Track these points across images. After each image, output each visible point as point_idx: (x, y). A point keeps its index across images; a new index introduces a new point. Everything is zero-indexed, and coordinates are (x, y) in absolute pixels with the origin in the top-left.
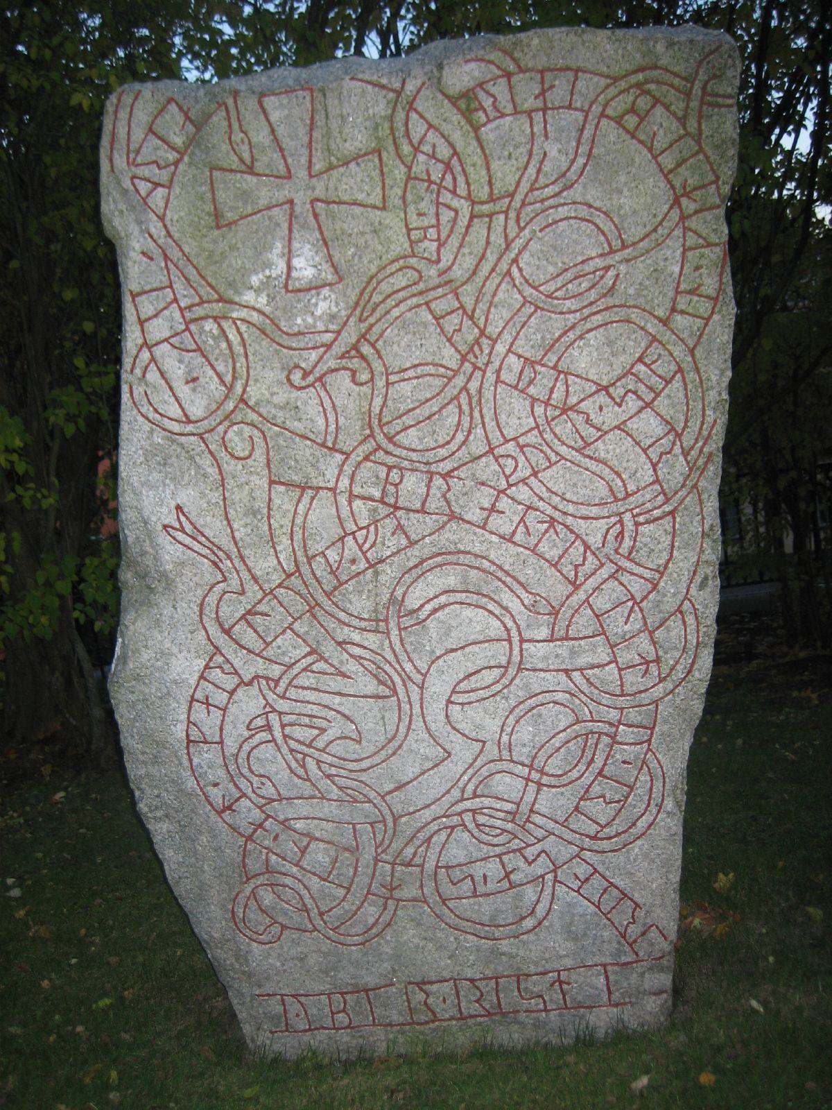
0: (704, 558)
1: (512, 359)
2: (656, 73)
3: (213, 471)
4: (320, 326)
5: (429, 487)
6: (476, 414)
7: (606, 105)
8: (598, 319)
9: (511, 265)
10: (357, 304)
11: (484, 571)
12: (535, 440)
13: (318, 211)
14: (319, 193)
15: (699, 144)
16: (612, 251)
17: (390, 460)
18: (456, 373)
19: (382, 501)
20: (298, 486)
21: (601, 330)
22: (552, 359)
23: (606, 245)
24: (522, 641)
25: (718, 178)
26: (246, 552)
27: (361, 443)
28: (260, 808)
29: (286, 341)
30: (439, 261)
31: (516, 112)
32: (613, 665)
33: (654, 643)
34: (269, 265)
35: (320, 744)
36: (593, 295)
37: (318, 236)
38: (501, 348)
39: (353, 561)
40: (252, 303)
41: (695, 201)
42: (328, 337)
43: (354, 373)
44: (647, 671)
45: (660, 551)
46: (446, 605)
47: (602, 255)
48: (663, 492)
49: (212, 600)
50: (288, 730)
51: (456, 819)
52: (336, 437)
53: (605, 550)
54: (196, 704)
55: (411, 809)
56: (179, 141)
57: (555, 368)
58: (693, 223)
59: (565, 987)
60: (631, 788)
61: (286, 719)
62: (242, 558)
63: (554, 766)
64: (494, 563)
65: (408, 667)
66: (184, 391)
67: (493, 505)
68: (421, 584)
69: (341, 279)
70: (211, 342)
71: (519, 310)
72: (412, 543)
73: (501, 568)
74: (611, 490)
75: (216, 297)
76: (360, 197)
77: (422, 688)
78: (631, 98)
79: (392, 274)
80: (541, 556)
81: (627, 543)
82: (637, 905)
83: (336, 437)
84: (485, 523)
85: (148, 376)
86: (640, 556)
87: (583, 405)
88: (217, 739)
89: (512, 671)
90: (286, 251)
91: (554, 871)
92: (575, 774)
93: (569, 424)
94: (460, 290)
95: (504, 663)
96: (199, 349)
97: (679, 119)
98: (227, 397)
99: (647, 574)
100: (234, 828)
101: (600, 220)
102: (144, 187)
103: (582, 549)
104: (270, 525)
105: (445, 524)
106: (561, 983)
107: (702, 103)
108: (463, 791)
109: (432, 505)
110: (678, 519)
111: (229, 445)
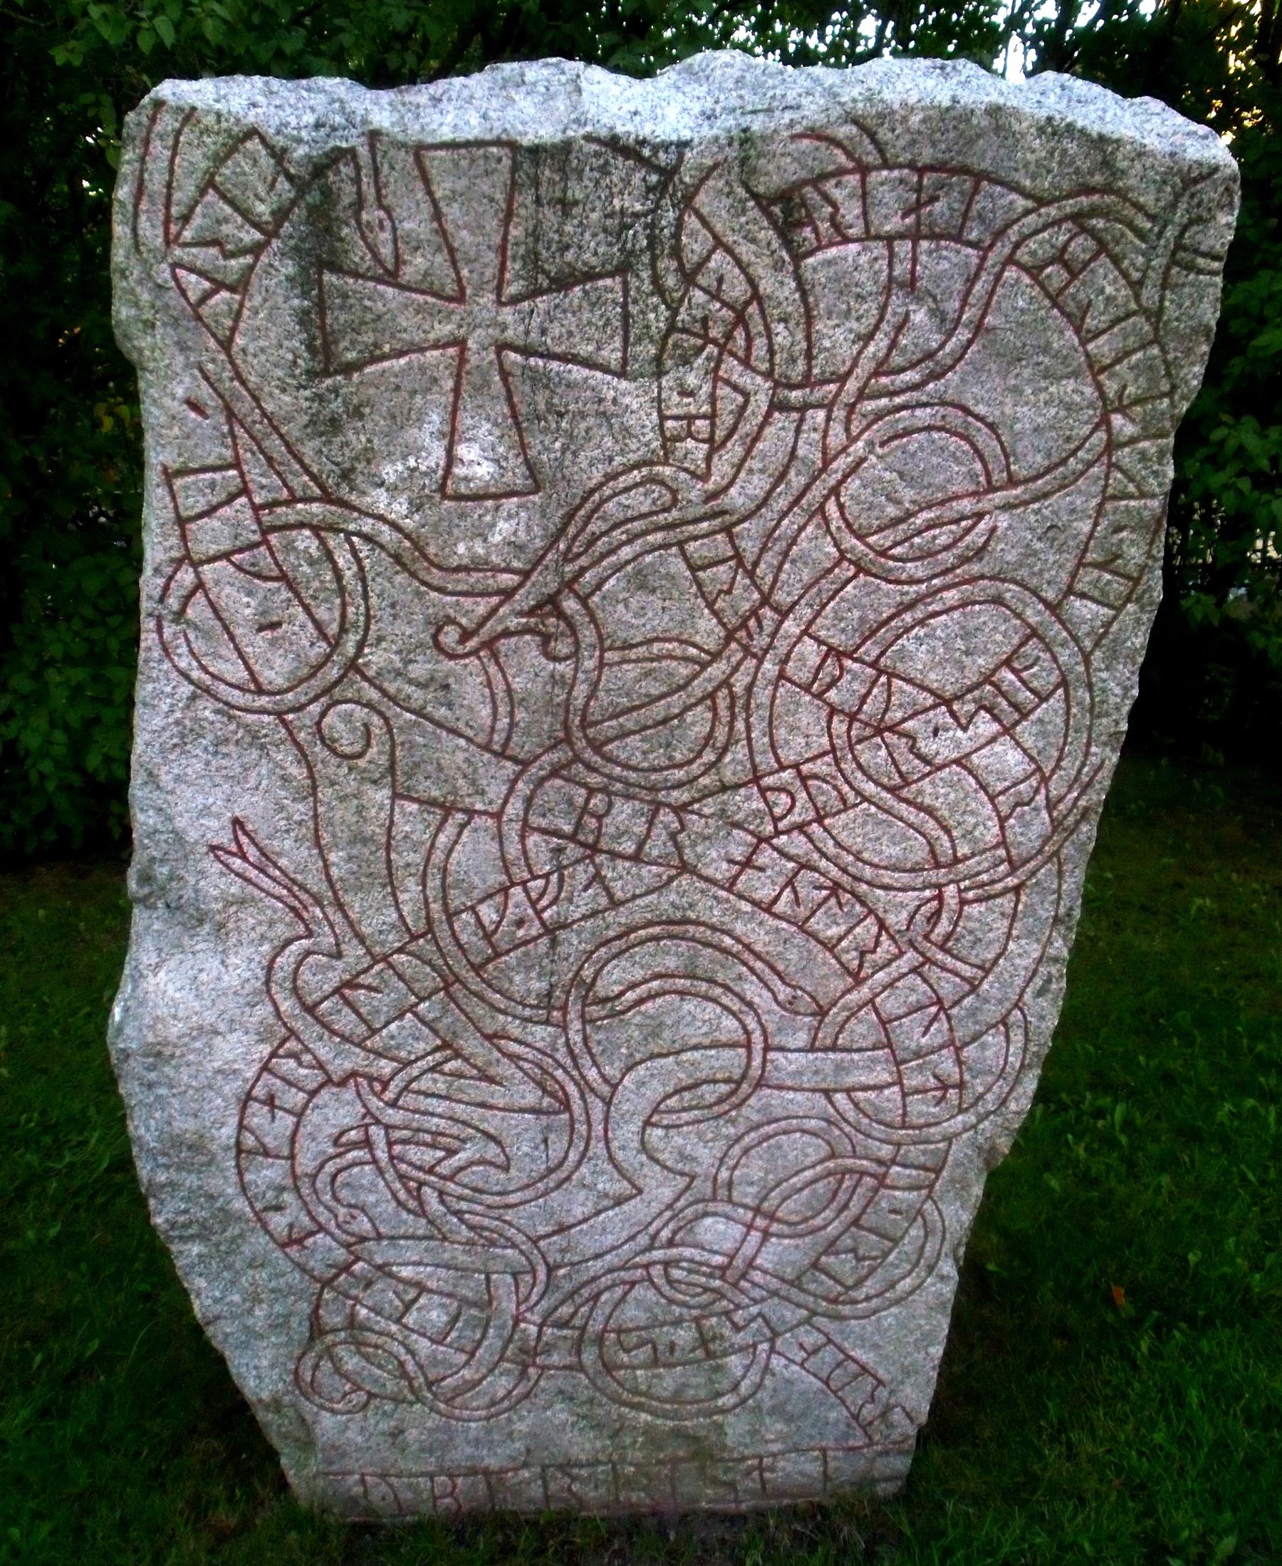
0: (1052, 951)
1: (808, 645)
2: (1110, 199)
4: (495, 559)
5: (651, 823)
6: (740, 725)
7: (1017, 246)
8: (952, 596)
10: (562, 531)
11: (725, 951)
13: (507, 367)
15: (1156, 329)
16: (991, 489)
17: (594, 780)
18: (715, 656)
19: (572, 837)
20: (442, 806)
21: (956, 614)
22: (870, 650)
24: (767, 1049)
25: (1174, 388)
26: (346, 898)
27: (552, 748)
28: (348, 1246)
29: (436, 576)
30: (705, 477)
31: (868, 236)
32: (896, 1089)
33: (959, 1062)
34: (417, 450)
35: (444, 1169)
36: (948, 558)
37: (506, 410)
38: (791, 627)
39: (520, 923)
40: (381, 508)
41: (1133, 421)
42: (507, 579)
43: (546, 639)
44: (943, 1097)
45: (990, 942)
47: (974, 494)
49: (286, 961)
50: (397, 1149)
51: (639, 1273)
52: (508, 738)
53: (910, 934)
54: (255, 1106)
57: (873, 665)
58: (1124, 456)
60: (896, 1242)
61: (397, 1134)
62: (340, 907)
63: (789, 1210)
64: (738, 940)
65: (592, 1074)
66: (256, 644)
70: (306, 569)
71: (830, 571)
72: (615, 904)
73: (748, 947)
74: (933, 852)
76: (586, 349)
77: (608, 1103)
78: (1063, 238)
79: (627, 490)
80: (813, 935)
81: (943, 927)
82: (880, 1382)
83: (508, 738)
84: (733, 884)
85: (190, 612)
86: (962, 947)
87: (909, 725)
88: (286, 1152)
90: (447, 429)
91: (772, 1341)
92: (818, 1221)
93: (883, 752)
94: (737, 529)
96: (283, 577)
98: (328, 658)
100: (303, 1269)
101: (983, 438)
103: (875, 929)
104: (389, 861)
105: (671, 879)
107: (1173, 261)
108: (654, 1237)
109: (654, 849)
111: (326, 731)
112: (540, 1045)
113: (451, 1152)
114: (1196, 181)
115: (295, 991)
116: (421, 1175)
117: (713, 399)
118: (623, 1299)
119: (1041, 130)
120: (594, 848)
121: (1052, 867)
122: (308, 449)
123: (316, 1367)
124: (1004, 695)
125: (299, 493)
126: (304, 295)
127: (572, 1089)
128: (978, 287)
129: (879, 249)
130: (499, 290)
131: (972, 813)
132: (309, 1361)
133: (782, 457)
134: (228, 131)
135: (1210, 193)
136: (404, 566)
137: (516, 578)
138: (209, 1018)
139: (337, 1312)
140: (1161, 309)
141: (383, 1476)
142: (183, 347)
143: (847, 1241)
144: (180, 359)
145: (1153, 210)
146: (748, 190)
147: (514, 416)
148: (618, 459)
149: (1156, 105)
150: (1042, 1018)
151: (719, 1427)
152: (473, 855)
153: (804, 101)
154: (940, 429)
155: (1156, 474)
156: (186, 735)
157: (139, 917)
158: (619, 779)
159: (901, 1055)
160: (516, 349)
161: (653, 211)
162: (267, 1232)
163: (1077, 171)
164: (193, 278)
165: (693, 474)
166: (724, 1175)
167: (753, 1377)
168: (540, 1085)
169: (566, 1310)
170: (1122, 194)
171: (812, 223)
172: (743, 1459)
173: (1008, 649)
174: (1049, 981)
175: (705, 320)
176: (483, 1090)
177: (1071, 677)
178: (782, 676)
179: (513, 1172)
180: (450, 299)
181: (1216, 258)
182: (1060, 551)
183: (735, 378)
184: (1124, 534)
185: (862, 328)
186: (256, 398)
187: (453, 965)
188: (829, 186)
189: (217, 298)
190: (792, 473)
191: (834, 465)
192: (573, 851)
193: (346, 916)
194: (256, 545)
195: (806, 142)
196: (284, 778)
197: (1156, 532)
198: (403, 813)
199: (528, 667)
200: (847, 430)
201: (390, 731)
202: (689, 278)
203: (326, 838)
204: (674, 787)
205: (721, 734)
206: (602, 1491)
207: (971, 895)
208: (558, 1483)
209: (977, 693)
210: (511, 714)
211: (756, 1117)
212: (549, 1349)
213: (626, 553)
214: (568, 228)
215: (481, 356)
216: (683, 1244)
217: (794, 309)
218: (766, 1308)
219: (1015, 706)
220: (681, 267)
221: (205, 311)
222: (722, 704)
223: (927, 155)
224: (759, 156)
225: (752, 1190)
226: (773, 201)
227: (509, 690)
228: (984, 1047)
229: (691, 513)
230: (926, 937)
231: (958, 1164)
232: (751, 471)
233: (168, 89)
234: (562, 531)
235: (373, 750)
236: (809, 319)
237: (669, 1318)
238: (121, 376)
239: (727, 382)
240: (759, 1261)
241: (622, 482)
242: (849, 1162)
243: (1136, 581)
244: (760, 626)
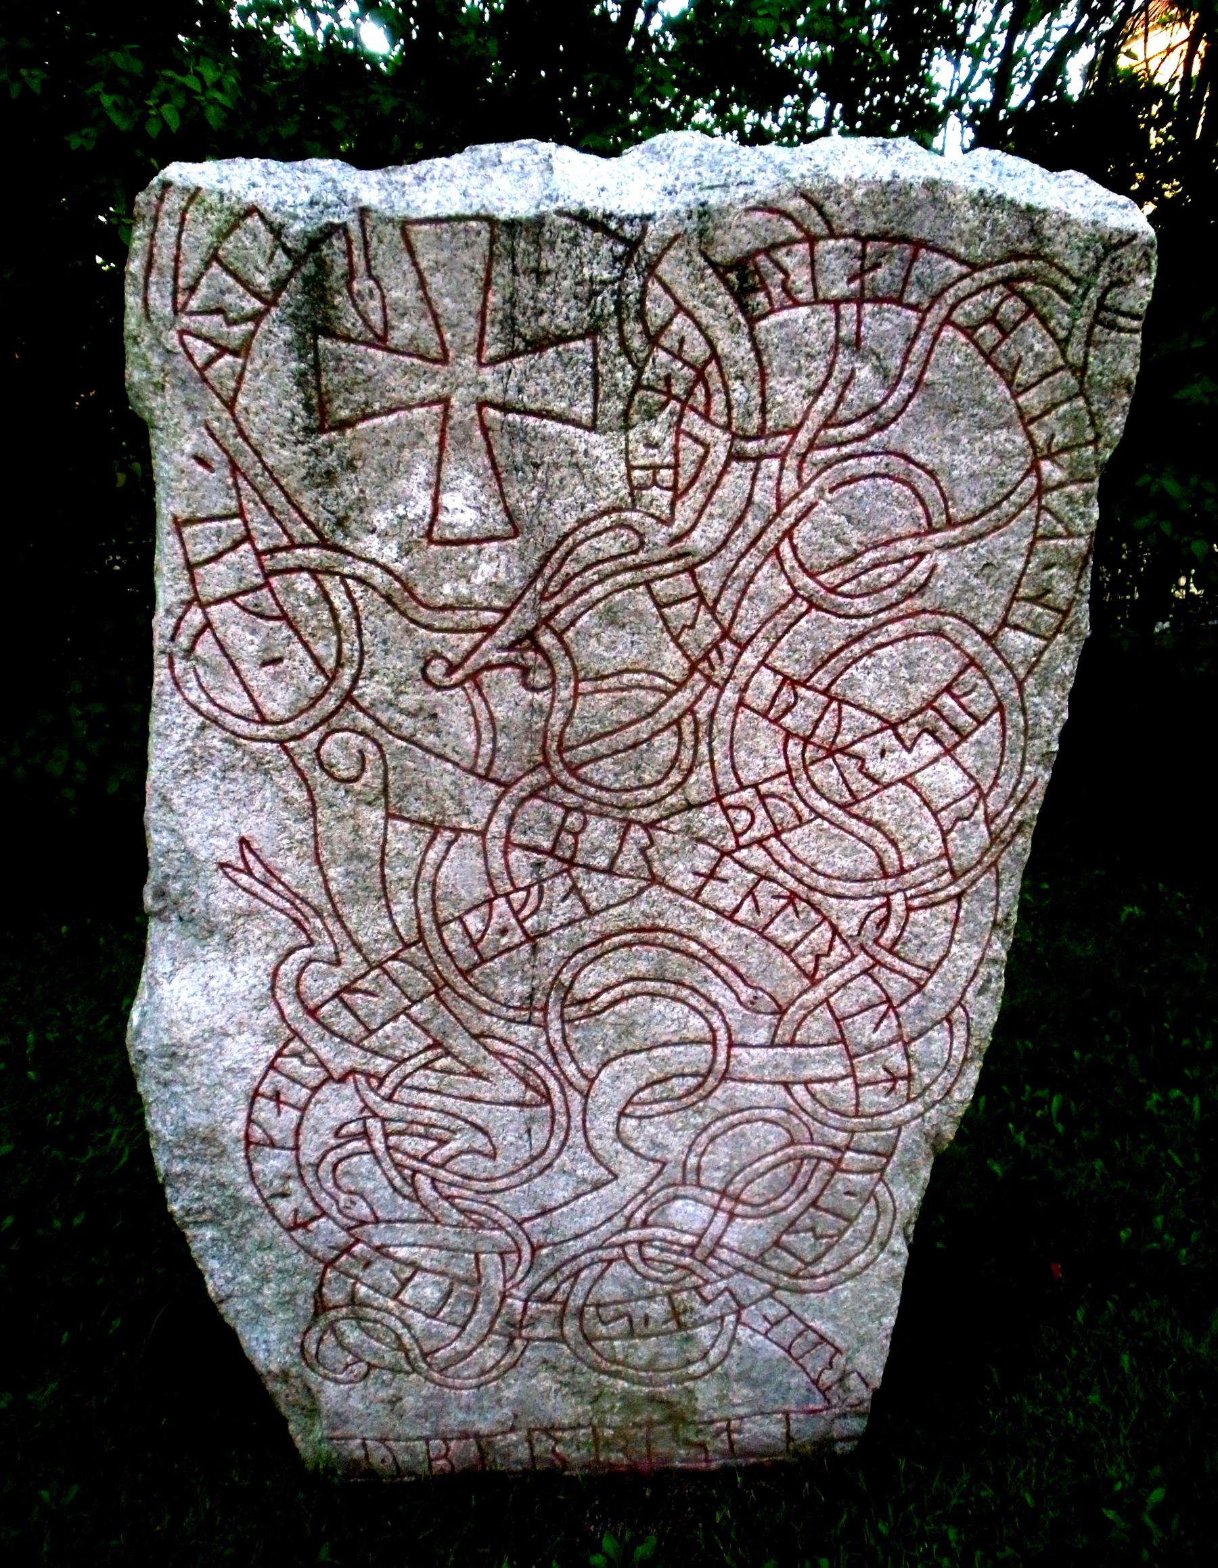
0: (990, 954)
1: (765, 676)
2: (1036, 264)
3: (299, 795)
4: (478, 598)
5: (623, 839)
6: (703, 749)
7: (953, 308)
9: (781, 540)
10: (538, 572)
11: (692, 956)
12: (782, 789)
15: (1081, 383)
16: (932, 530)
17: (570, 800)
18: (680, 686)
19: (551, 853)
20: (431, 825)
21: (901, 645)
22: (822, 679)
23: (923, 521)
24: (731, 1045)
25: (1098, 437)
26: (344, 910)
28: (348, 1229)
29: (424, 615)
30: (669, 522)
31: (817, 300)
32: (850, 1081)
33: (907, 1056)
35: (436, 1158)
36: (893, 594)
37: (487, 462)
38: (749, 658)
39: (504, 932)
40: (373, 554)
41: (1060, 467)
42: (489, 617)
43: (525, 671)
44: (893, 1089)
46: (630, 996)
48: (952, 870)
49: (289, 968)
50: (393, 1140)
51: (616, 1252)
52: (491, 763)
56: (263, 281)
57: (825, 692)
60: (850, 1221)
62: (339, 918)
64: (704, 946)
65: (571, 1069)
66: (259, 678)
67: (713, 871)
69: (516, 534)
70: (305, 609)
71: (784, 607)
72: (590, 913)
73: (712, 952)
74: (881, 864)
75: (315, 538)
76: (559, 406)
79: (598, 534)
80: (771, 940)
81: (892, 932)
82: (838, 1350)
83: (491, 763)
85: (199, 650)
86: (908, 950)
87: (858, 748)
88: (291, 1144)
90: (432, 479)
91: (738, 1313)
92: (780, 1203)
93: (835, 772)
94: (699, 570)
96: (284, 616)
97: (1058, 342)
98: (326, 690)
100: (308, 1251)
101: (923, 483)
102: (203, 352)
103: (829, 935)
104: (383, 876)
105: (641, 890)
107: (1096, 320)
108: (629, 1219)
109: (626, 862)
110: (965, 905)
111: (324, 758)
112: (523, 1043)
113: (442, 1142)
115: (298, 994)
116: (415, 1164)
117: (676, 450)
118: (601, 1276)
119: (974, 202)
120: (571, 863)
122: (306, 499)
123: (320, 1341)
124: (944, 718)
125: (298, 540)
126: (301, 358)
127: (552, 1084)
128: (918, 346)
129: (827, 312)
130: (479, 351)
131: (917, 827)
132: (314, 1334)
133: (739, 503)
134: (230, 209)
135: (1129, 258)
136: (394, 605)
137: (498, 616)
138: (220, 1021)
139: (340, 1290)
140: (1086, 364)
141: (383, 1440)
142: (190, 407)
143: (806, 1221)
144: (188, 419)
145: (1076, 272)
146: (707, 259)
147: (494, 466)
148: (589, 506)
149: (1079, 178)
150: (983, 1015)
151: (690, 1392)
152: (461, 870)
153: (758, 177)
154: (884, 476)
155: (1082, 515)
156: (197, 761)
157: (155, 929)
158: (592, 799)
159: (854, 1049)
160: (495, 406)
161: (620, 279)
162: (274, 1217)
163: (1007, 239)
164: (199, 343)
165: (659, 520)
166: (693, 1160)
167: (721, 1346)
168: (523, 1080)
169: (548, 1287)
170: (1049, 260)
171: (765, 288)
172: (712, 1422)
173: (949, 677)
174: (989, 981)
175: (668, 379)
176: (472, 1085)
177: (1006, 702)
178: (741, 703)
179: (499, 1160)
181: (1135, 317)
182: (995, 587)
183: (696, 431)
184: (1054, 571)
185: (812, 384)
186: (257, 453)
187: (444, 972)
188: (780, 255)
189: (221, 362)
190: (749, 518)
191: (788, 510)
192: (551, 865)
193: (344, 927)
194: (258, 588)
195: (759, 214)
196: (286, 801)
197: (1083, 569)
198: (396, 832)
199: (508, 696)
200: (799, 477)
201: (383, 757)
202: (653, 339)
203: (325, 856)
205: (686, 757)
206: (584, 1452)
207: (916, 902)
208: (543, 1445)
209: (920, 717)
210: (494, 740)
211: (721, 1108)
213: (598, 591)
214: (542, 295)
215: (462, 413)
216: (655, 1225)
221: (210, 373)
222: (687, 729)
223: (869, 225)
224: (716, 228)
225: (720, 1174)
227: (492, 718)
228: (929, 1041)
229: (657, 555)
230: (876, 941)
231: (907, 1150)
232: (711, 516)
233: (176, 172)
234: (538, 572)
235: (368, 775)
236: (763, 376)
238: (135, 435)
239: (689, 435)
240: (725, 1240)
241: (594, 527)
242: (807, 1148)
243: (1065, 614)
244: (721, 657)
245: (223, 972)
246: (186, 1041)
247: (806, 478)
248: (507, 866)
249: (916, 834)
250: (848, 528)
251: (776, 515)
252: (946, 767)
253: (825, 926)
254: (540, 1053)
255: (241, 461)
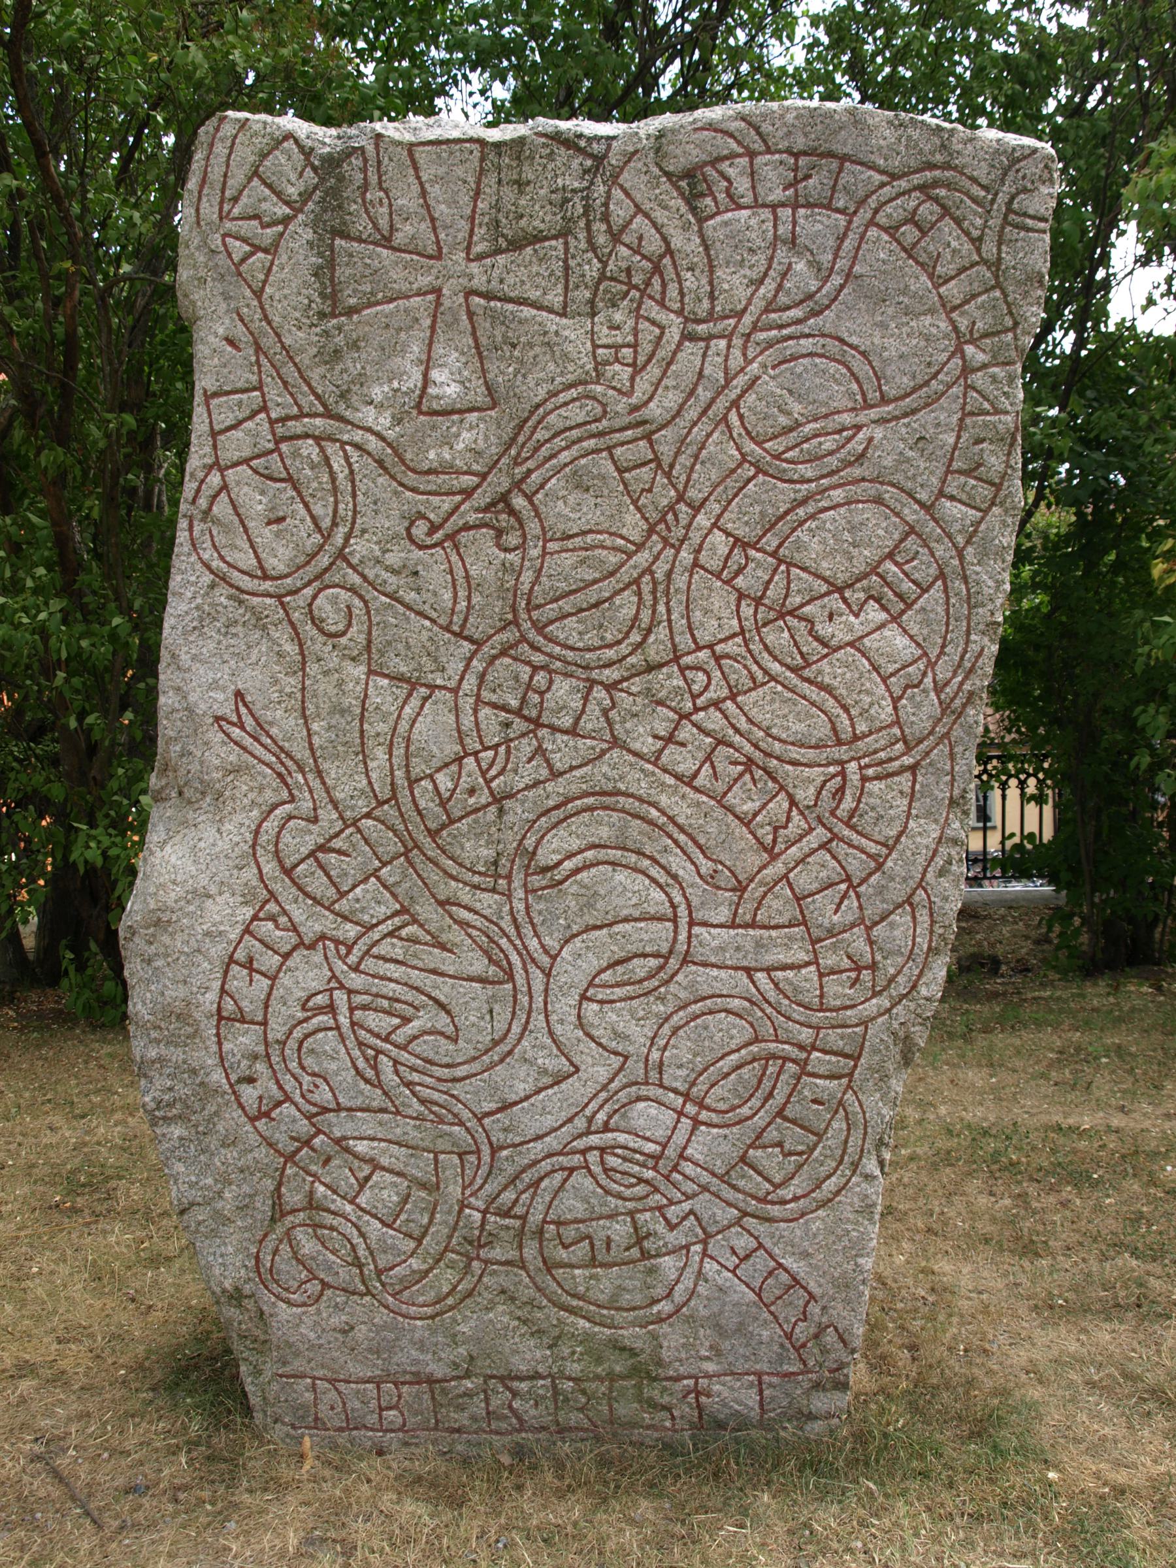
0: (949, 832)
1: (718, 537)
3: (291, 648)
5: (586, 699)
6: (661, 608)
8: (838, 495)
10: (513, 440)
11: (651, 823)
14: (479, 282)
15: (997, 277)
17: (538, 658)
18: (640, 547)
19: (518, 713)
20: (408, 681)
21: (842, 510)
22: (770, 542)
24: (692, 923)
25: (1016, 324)
26: (325, 766)
28: (309, 1118)
29: (411, 479)
30: (629, 394)
31: (757, 204)
32: (813, 968)
33: (871, 943)
34: (398, 375)
35: (400, 1037)
36: (833, 462)
38: (703, 520)
39: (472, 792)
40: (370, 422)
42: (469, 480)
43: (500, 533)
45: (892, 819)
46: (592, 865)
47: (853, 409)
49: (271, 825)
51: (577, 1159)
54: (235, 968)
55: (518, 1140)
56: (292, 191)
57: (774, 554)
58: (978, 379)
59: (703, 1399)
60: (820, 1136)
61: (358, 999)
62: (319, 773)
64: (664, 813)
65: (533, 944)
66: (264, 535)
67: (672, 735)
68: (561, 831)
70: (308, 472)
71: (733, 471)
72: (555, 774)
73: (671, 819)
74: (834, 729)
76: (534, 294)
78: (913, 204)
79: (566, 404)
80: (729, 809)
81: (848, 803)
82: (812, 1296)
83: (466, 620)
87: (807, 609)
89: (673, 963)
90: (424, 357)
91: (705, 1242)
92: (745, 1111)
93: (786, 634)
95: (664, 951)
96: (289, 479)
97: (973, 240)
98: (321, 547)
99: (873, 848)
101: (858, 364)
102: (239, 248)
103: (786, 805)
104: (362, 732)
105: (603, 752)
106: (698, 1394)
108: (590, 1120)
109: (589, 723)
110: (919, 778)
111: (316, 612)
112: (486, 912)
113: (406, 1020)
114: (1019, 160)
117: (635, 332)
118: (561, 1187)
120: (537, 723)
121: (944, 748)
122: (315, 375)
123: (276, 1252)
124: (888, 584)
125: (306, 410)
126: (320, 255)
128: (847, 243)
129: (766, 214)
130: (468, 249)
131: (868, 692)
132: (270, 1244)
136: (385, 469)
138: (203, 880)
139: (298, 1189)
140: (999, 259)
142: (227, 297)
143: (772, 1134)
144: (224, 306)
145: (984, 182)
147: (477, 347)
152: (433, 729)
156: (205, 617)
163: (921, 152)
165: (619, 391)
166: (655, 1055)
167: (687, 1282)
169: (509, 1196)
171: (712, 194)
173: (890, 543)
175: (628, 270)
178: (696, 564)
180: (430, 257)
182: (929, 459)
186: (278, 335)
187: (418, 836)
188: (724, 166)
190: (700, 389)
192: (519, 725)
193: (324, 783)
194: (271, 452)
197: (1012, 445)
198: (376, 687)
199: (483, 556)
201: (368, 613)
202: (616, 237)
203: (311, 709)
204: (605, 666)
210: (469, 598)
211: (683, 995)
212: (492, 1240)
213: (565, 456)
214: (523, 202)
215: (452, 300)
217: (700, 260)
218: (698, 1204)
219: (900, 596)
220: (610, 230)
222: (646, 588)
223: (800, 143)
225: (682, 1073)
226: (681, 178)
227: (467, 577)
228: (892, 925)
229: (618, 423)
230: (833, 813)
234: (513, 440)
235: (354, 629)
236: (712, 269)
237: (605, 1210)
239: (648, 319)
240: (689, 1151)
241: (563, 397)
243: (998, 487)
244: (677, 520)
245: (210, 833)
246: (171, 903)
247: (750, 355)
248: (477, 724)
249: (868, 699)
250: (790, 400)
251: (724, 388)
252: (892, 633)
253: (782, 795)
254: (503, 924)
255: (263, 342)
